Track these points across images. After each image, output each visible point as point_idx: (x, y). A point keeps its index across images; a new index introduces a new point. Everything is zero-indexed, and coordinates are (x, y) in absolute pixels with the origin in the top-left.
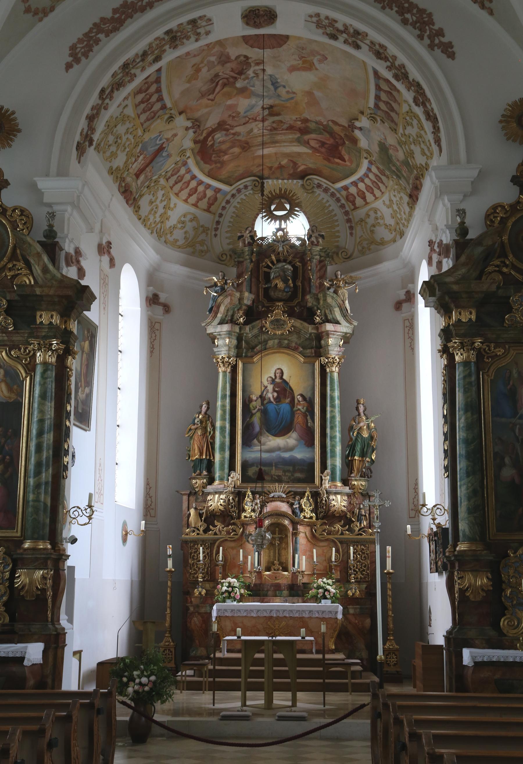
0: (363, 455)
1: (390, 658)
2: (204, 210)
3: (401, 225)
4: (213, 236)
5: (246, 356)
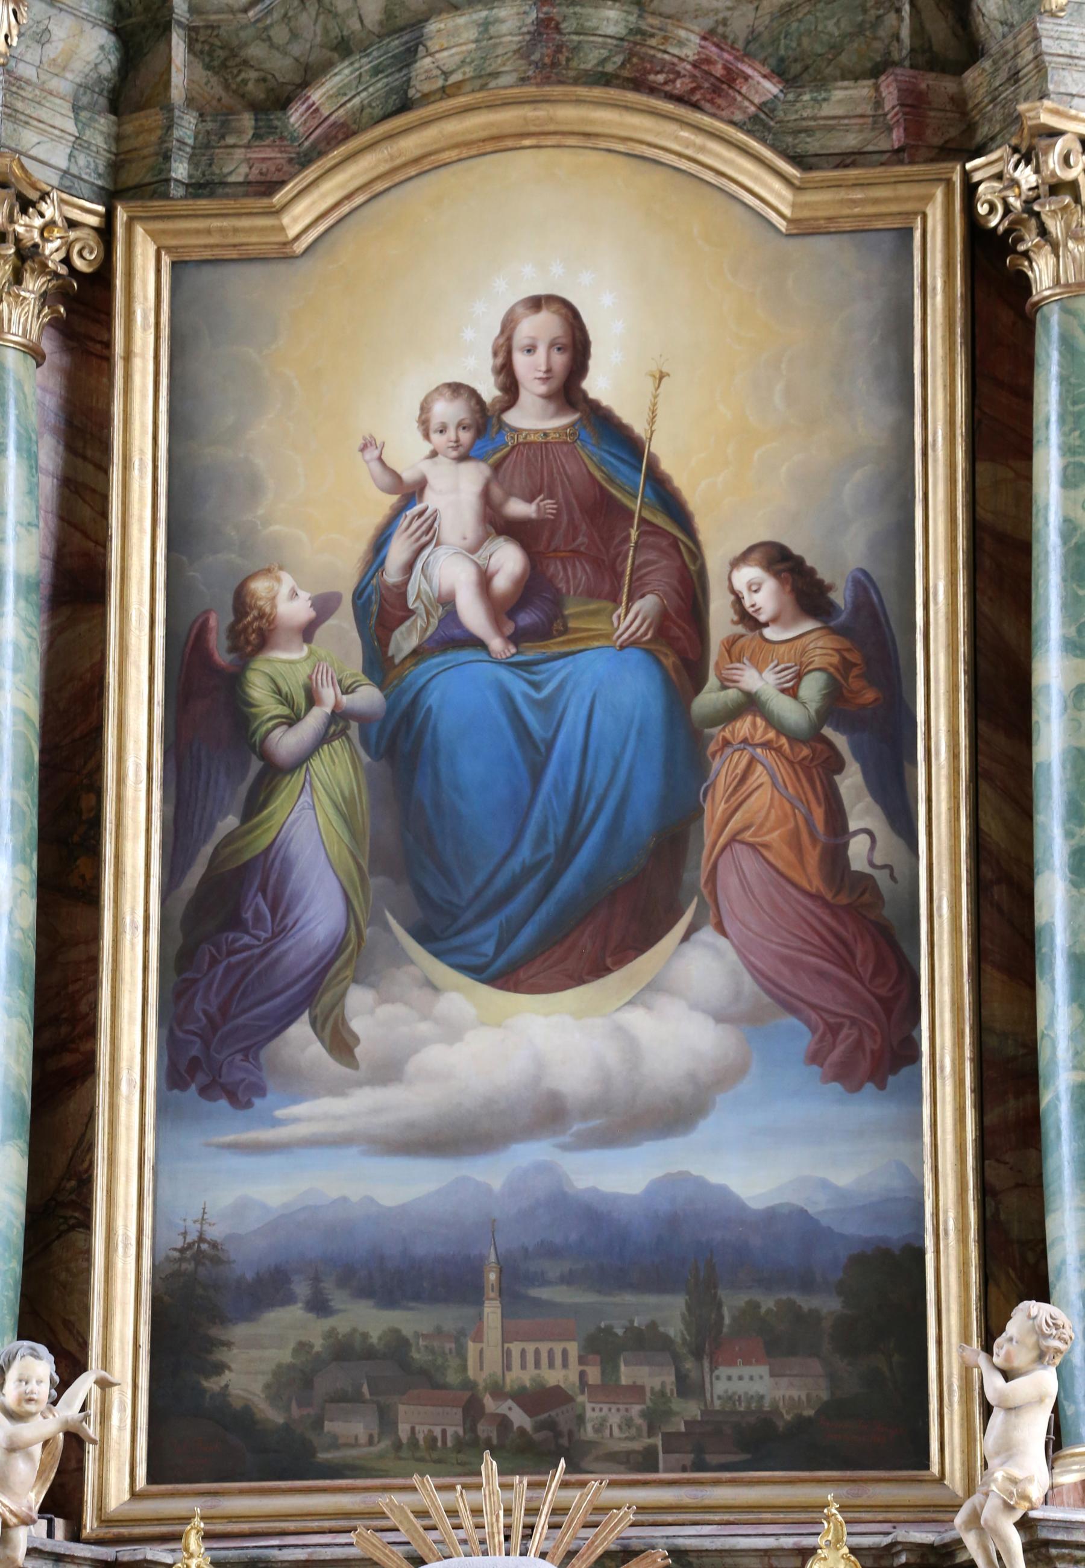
5: (200, 188)
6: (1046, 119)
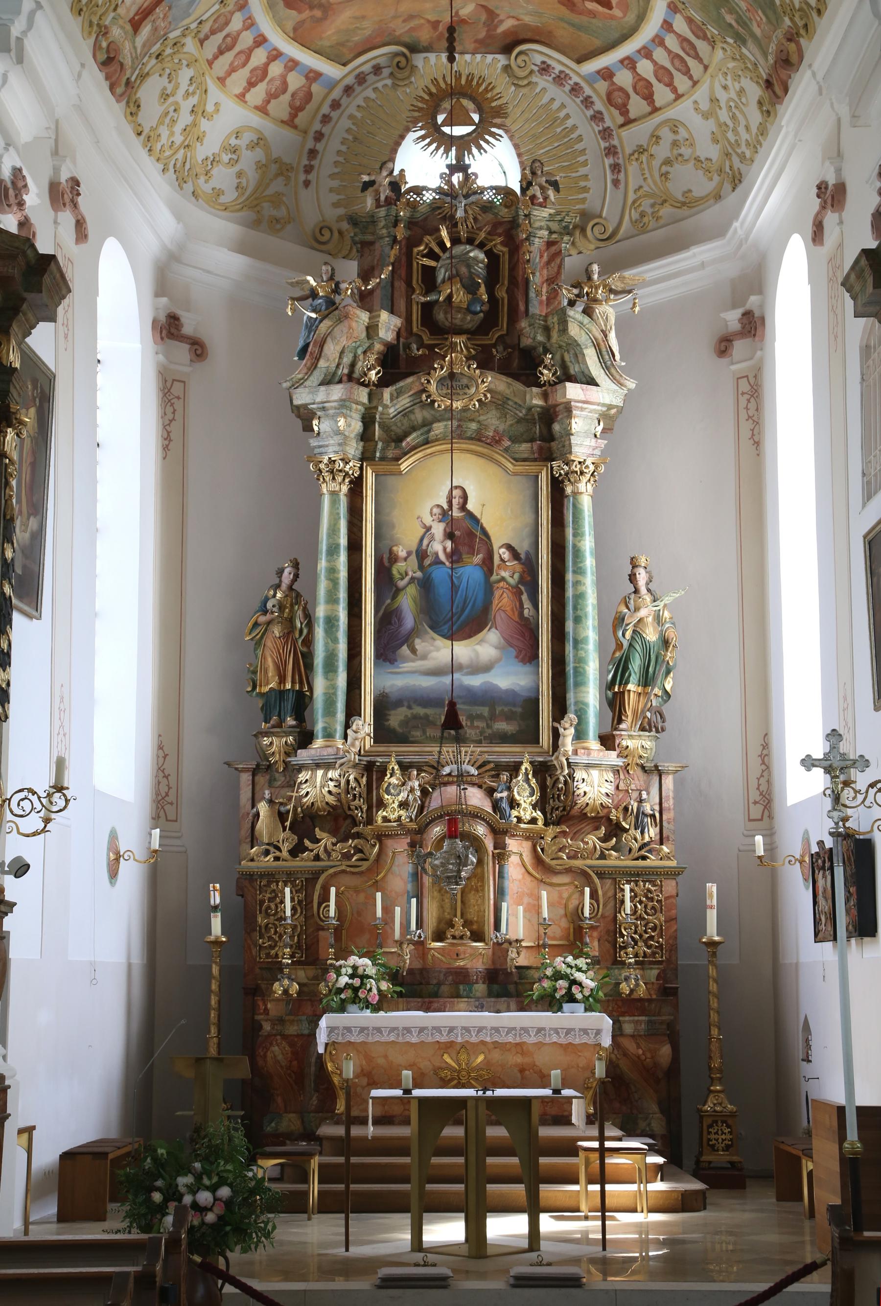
0: (646, 681)
1: (716, 1133)
3: (736, 160)
5: (382, 459)
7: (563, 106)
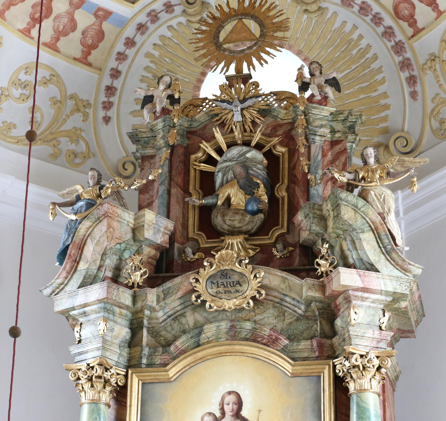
2: (75, 59)
4: (101, 120)
5: (150, 365)
6: (351, 350)
7: (355, 27)
